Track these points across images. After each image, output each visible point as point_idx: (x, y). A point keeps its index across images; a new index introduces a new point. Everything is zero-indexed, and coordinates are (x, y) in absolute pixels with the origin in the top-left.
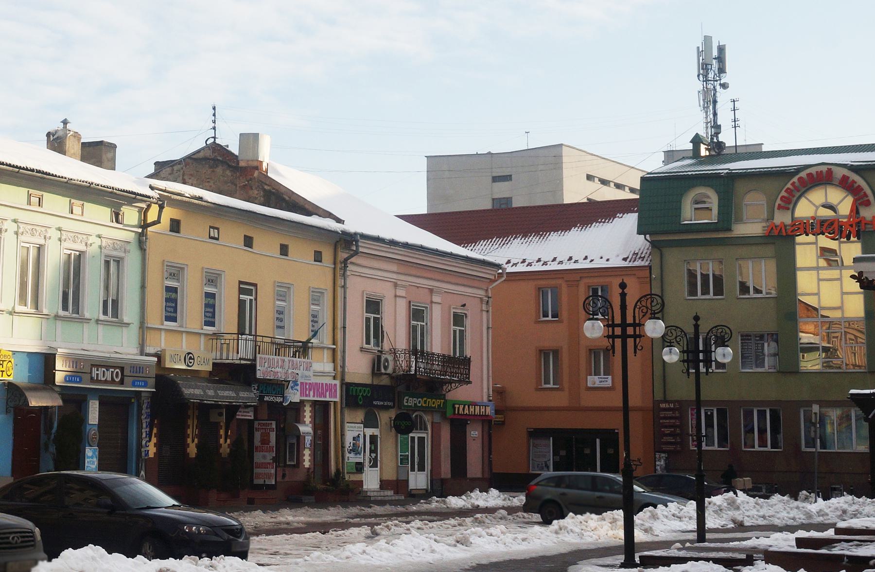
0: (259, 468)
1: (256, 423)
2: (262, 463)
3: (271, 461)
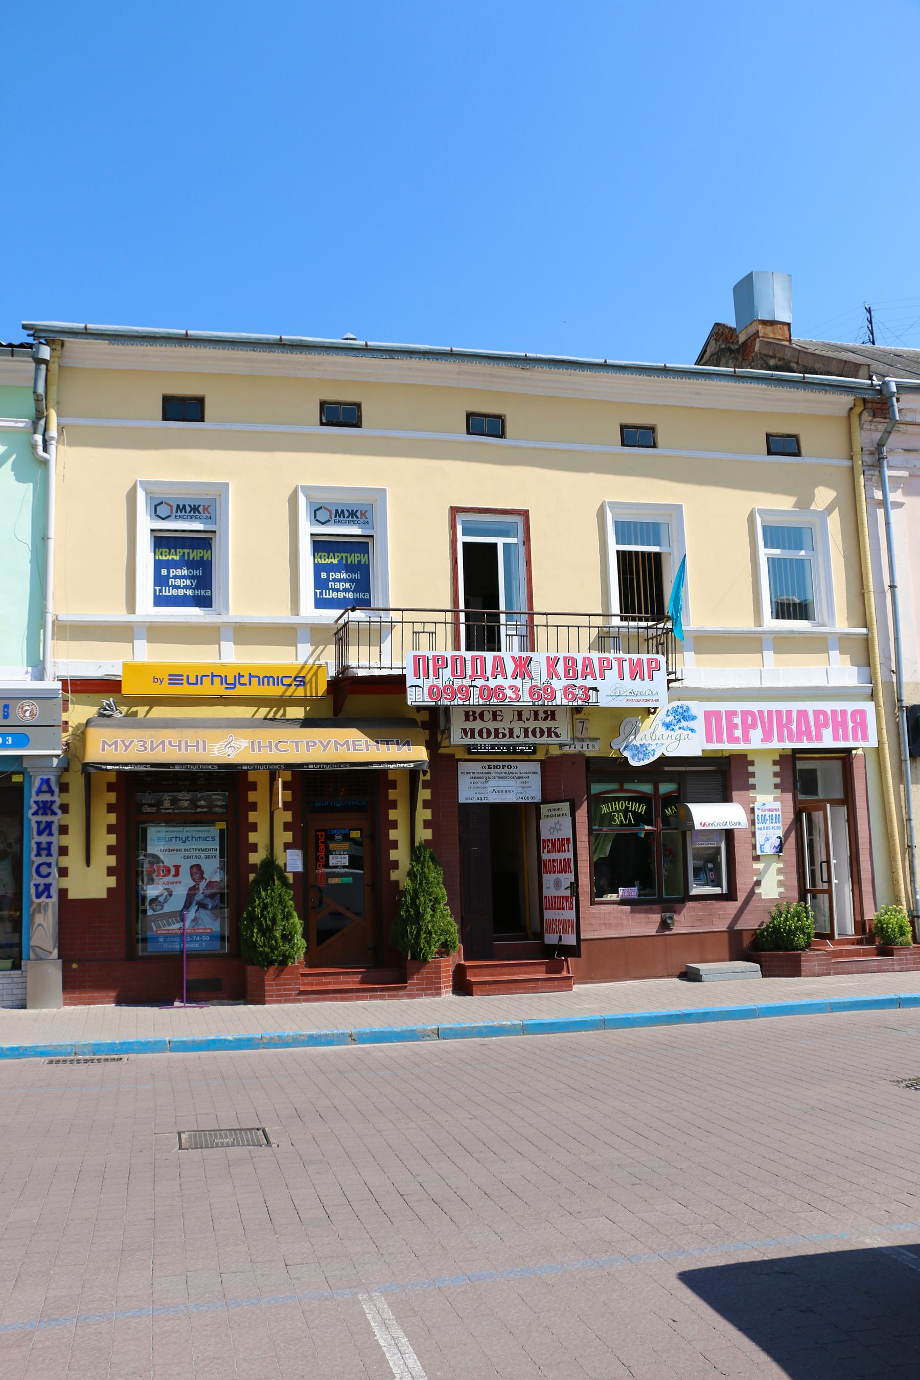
0: (550, 909)
1: (544, 808)
2: (555, 897)
3: (568, 893)
